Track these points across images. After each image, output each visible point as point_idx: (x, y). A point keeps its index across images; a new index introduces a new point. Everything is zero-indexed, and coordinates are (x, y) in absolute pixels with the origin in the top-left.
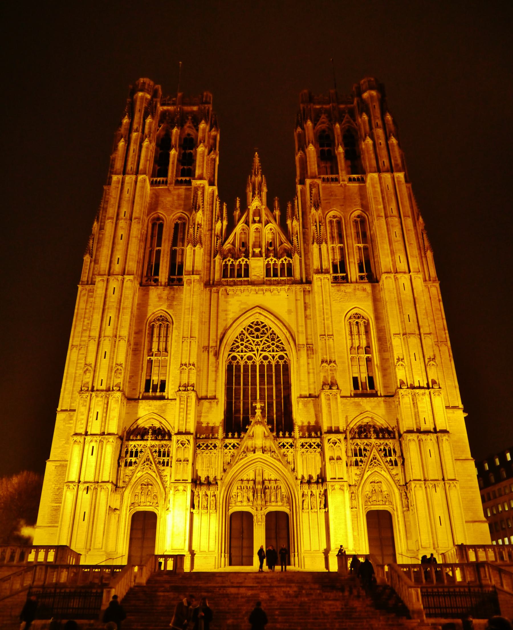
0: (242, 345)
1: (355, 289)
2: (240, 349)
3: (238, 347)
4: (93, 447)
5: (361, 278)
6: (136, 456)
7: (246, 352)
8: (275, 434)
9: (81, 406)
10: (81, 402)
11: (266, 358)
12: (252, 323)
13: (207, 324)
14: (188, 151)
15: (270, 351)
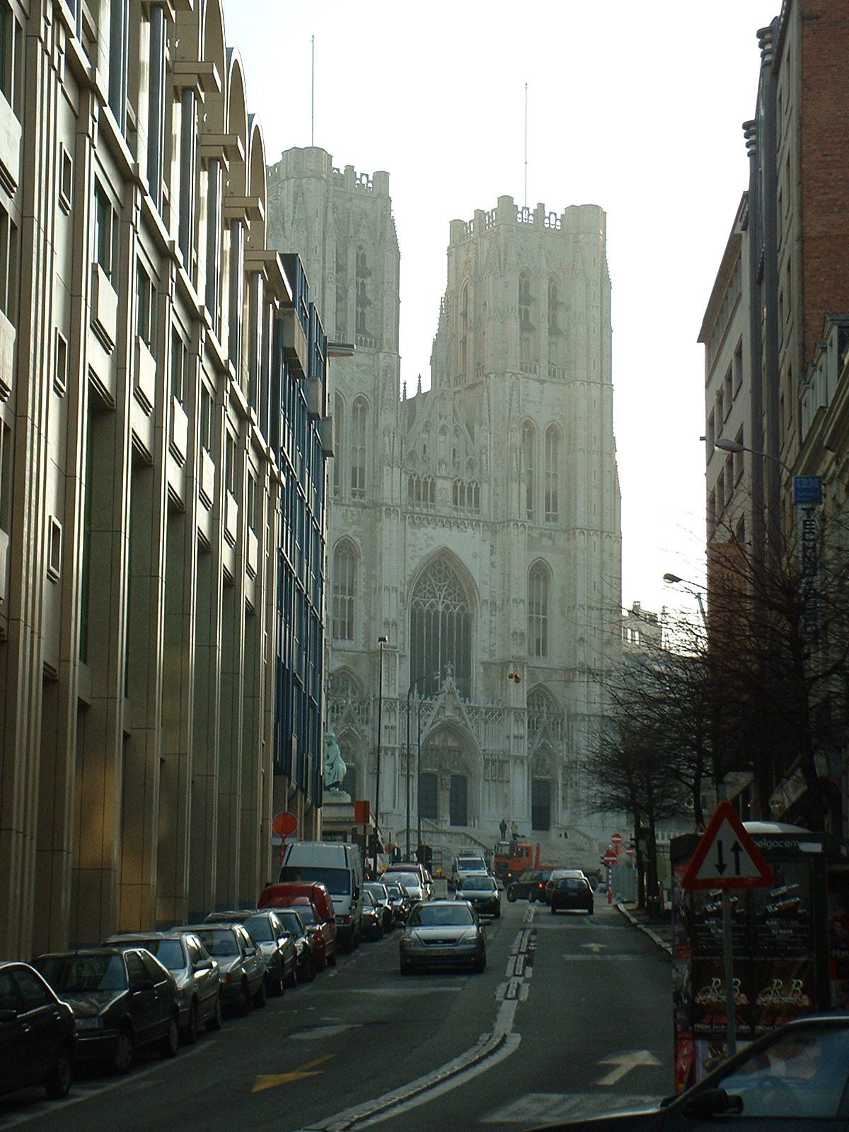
1: (542, 535)
3: (421, 591)
5: (547, 519)
6: (338, 712)
7: (428, 598)
8: (462, 699)
11: (447, 607)
12: (435, 562)
15: (451, 600)
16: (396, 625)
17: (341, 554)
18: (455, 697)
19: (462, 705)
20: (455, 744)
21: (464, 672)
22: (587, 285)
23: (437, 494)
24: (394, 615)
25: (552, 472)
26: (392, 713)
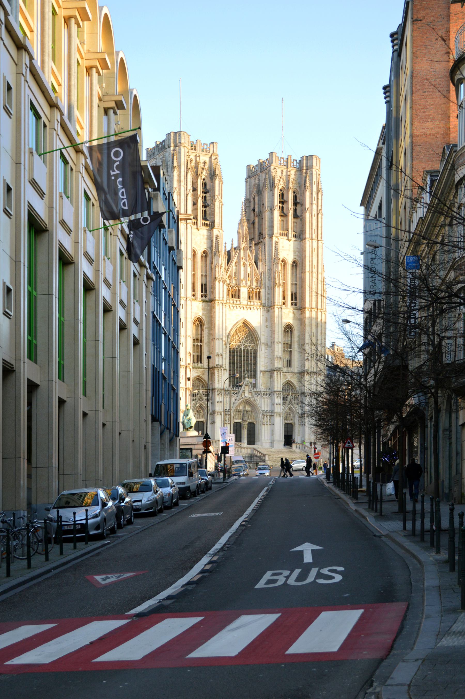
11: (246, 347)
19: (252, 390)
20: (249, 409)
21: (254, 376)
24: (221, 351)
25: (294, 283)
26: (220, 396)
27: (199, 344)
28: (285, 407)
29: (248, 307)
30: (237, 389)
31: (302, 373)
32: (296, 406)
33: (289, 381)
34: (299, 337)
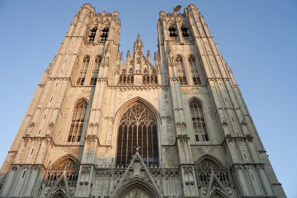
0: (128, 116)
1: (192, 88)
2: (127, 119)
3: (126, 118)
4: (25, 172)
6: (55, 180)
9: (23, 146)
10: (24, 143)
11: (142, 123)
13: (109, 105)
14: (105, 33)
16: (98, 126)
17: (80, 106)
18: (141, 164)
19: (146, 168)
22: (194, 19)
23: (134, 79)
24: (97, 121)
27: (80, 123)
28: (206, 191)
29: (142, 87)
30: (122, 167)
31: (224, 144)
32: (227, 188)
33: (207, 155)
34: (210, 108)
